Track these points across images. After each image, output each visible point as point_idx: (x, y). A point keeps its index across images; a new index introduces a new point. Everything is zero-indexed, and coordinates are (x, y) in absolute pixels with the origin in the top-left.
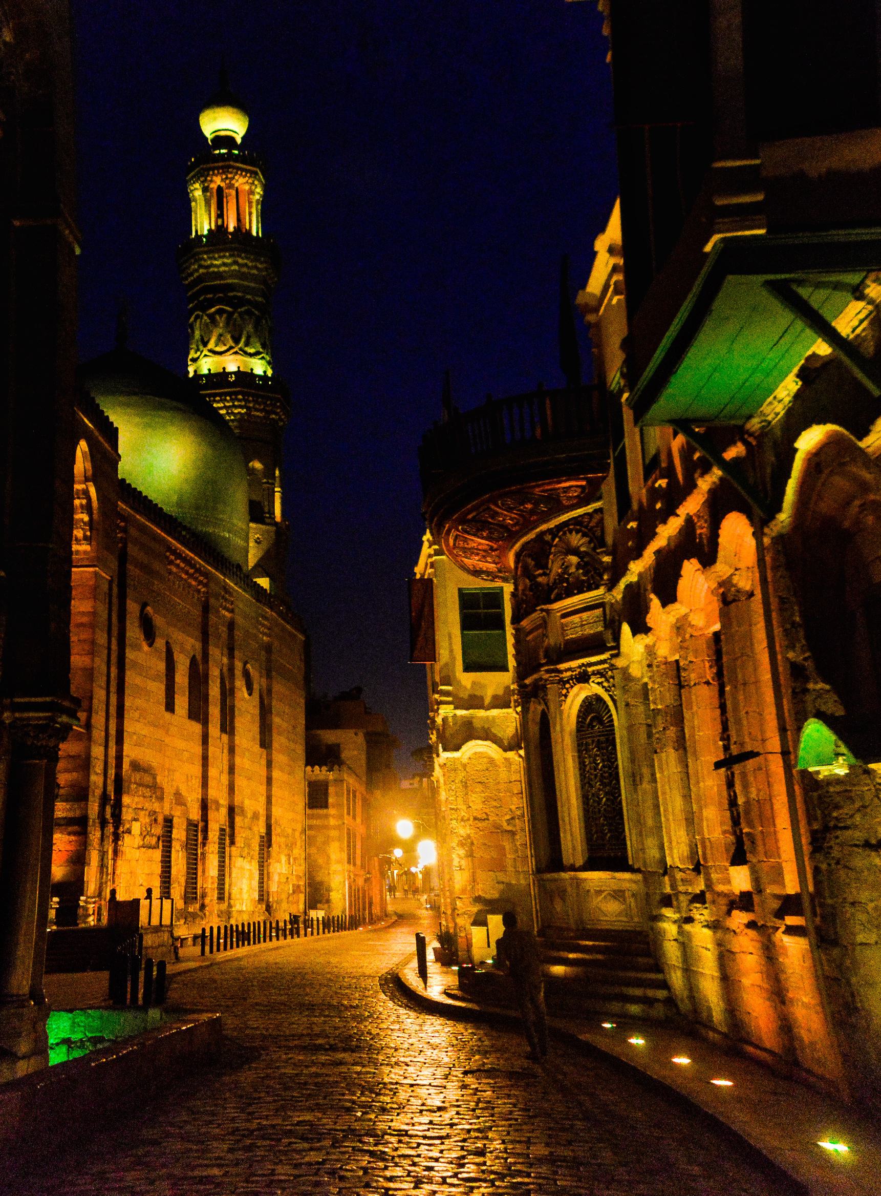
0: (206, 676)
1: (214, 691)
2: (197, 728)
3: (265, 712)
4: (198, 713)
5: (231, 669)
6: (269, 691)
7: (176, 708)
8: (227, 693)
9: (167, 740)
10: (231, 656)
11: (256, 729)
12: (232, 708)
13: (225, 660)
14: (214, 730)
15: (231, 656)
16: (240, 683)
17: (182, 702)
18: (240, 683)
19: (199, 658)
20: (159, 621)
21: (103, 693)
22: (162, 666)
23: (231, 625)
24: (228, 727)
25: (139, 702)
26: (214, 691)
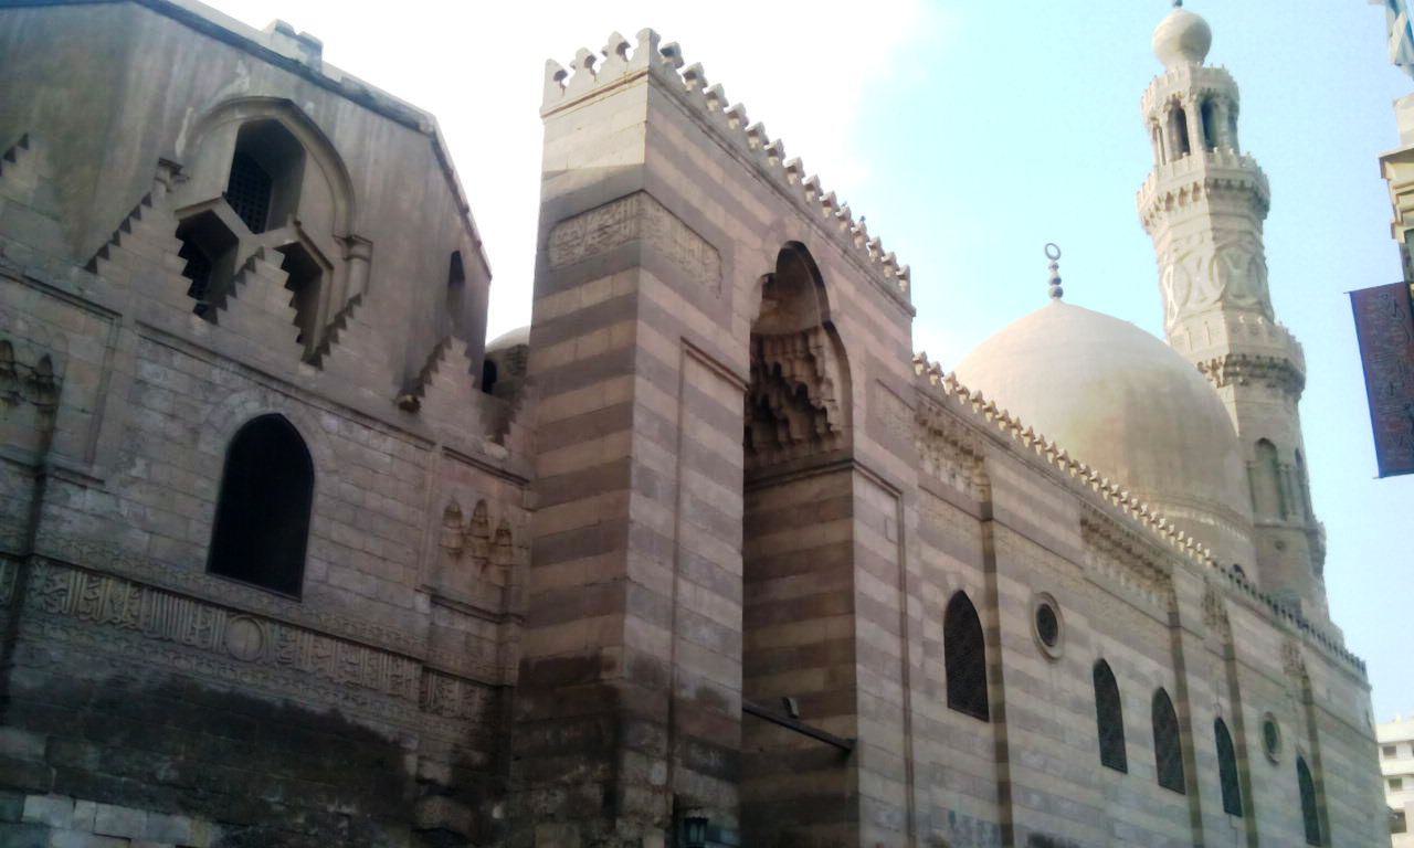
0: (1187, 720)
1: (1204, 743)
2: (1170, 799)
3: (1310, 789)
4: (1173, 770)
5: (1238, 720)
6: (1317, 760)
7: (1131, 764)
8: (1229, 752)
9: (1121, 812)
10: (1235, 696)
11: (1295, 811)
12: (1247, 776)
13: (1225, 703)
14: (1213, 805)
15: (1235, 696)
16: (1254, 739)
17: (1141, 754)
18: (1254, 739)
19: (1170, 690)
20: (1069, 618)
21: (893, 690)
22: (1087, 691)
23: (1229, 655)
24: (1236, 798)
25: (1039, 740)
26: (1204, 743)
